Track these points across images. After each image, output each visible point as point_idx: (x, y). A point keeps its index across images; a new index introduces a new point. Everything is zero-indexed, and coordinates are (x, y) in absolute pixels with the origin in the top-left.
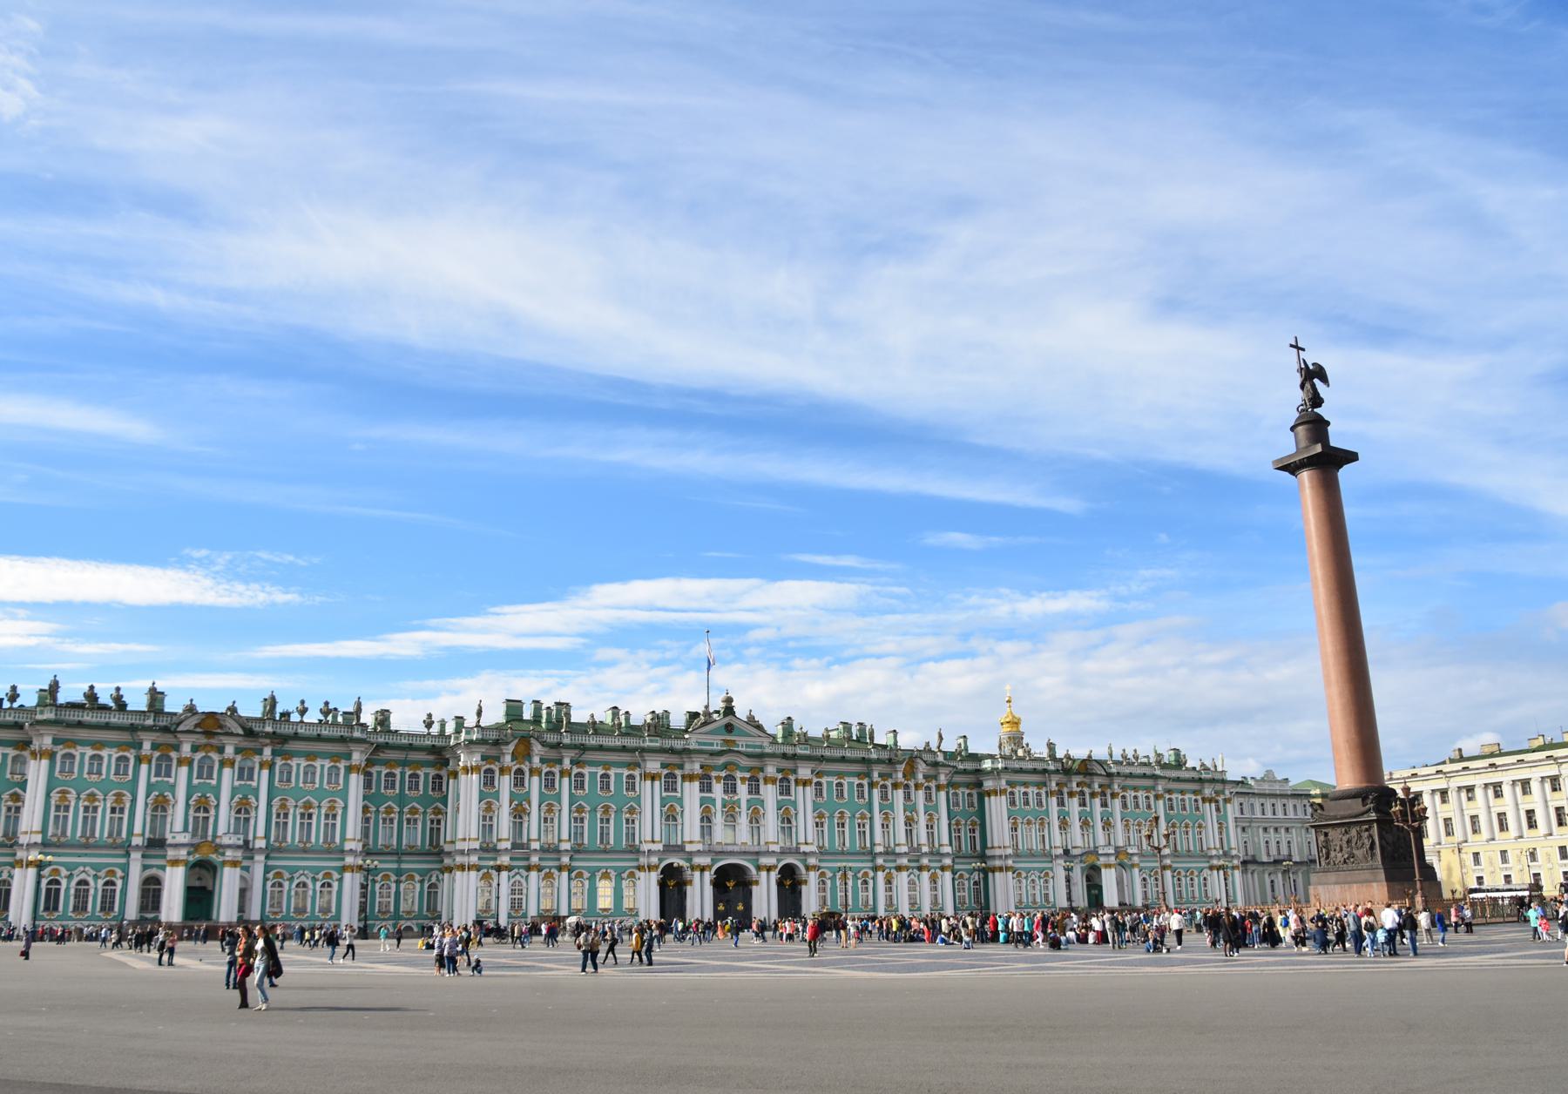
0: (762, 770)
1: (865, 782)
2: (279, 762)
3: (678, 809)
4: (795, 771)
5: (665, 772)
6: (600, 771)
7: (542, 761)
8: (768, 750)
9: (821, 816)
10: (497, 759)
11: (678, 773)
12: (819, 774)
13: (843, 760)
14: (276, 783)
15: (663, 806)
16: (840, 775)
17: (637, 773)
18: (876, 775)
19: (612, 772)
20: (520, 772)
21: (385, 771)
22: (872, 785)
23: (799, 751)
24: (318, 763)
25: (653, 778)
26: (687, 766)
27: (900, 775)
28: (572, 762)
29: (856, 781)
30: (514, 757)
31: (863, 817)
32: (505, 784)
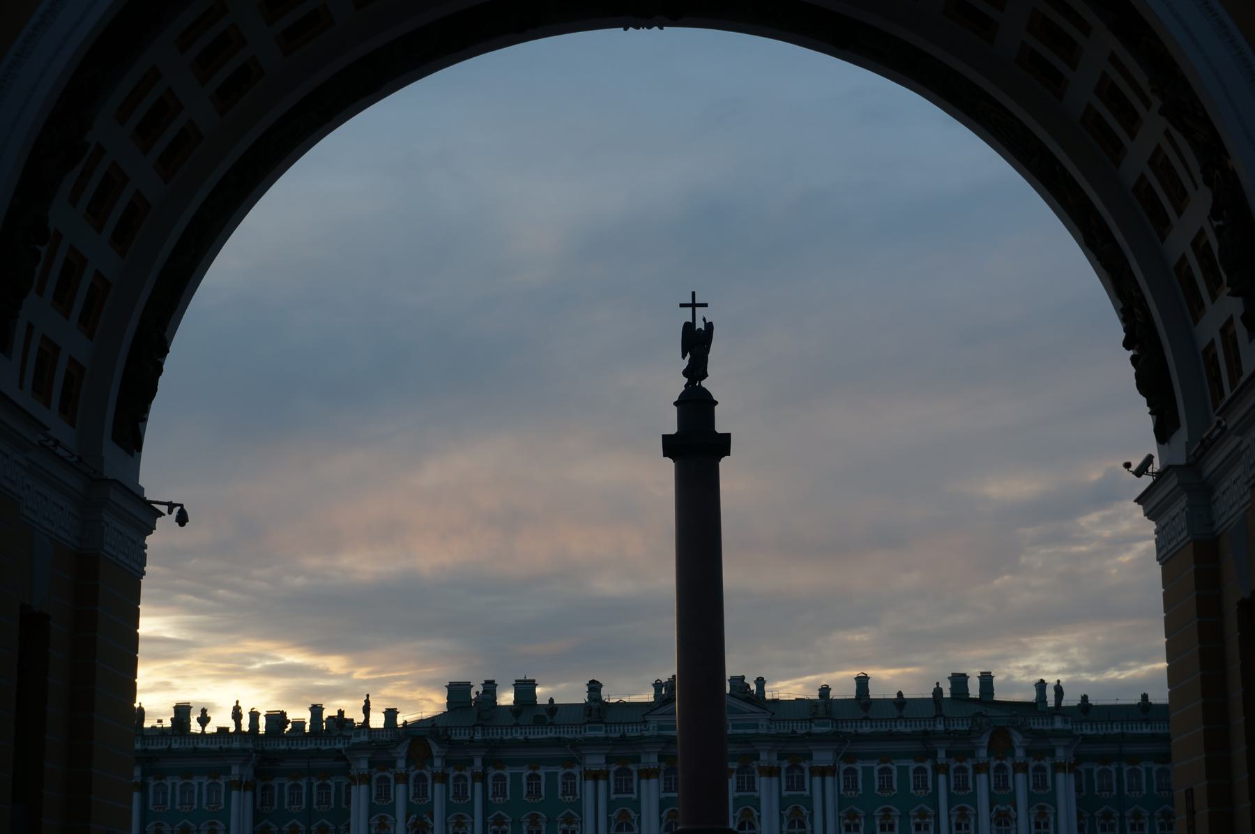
0: (757, 757)
1: (928, 765)
2: (152, 783)
3: (633, 814)
4: (809, 757)
5: (614, 768)
6: (526, 772)
7: (448, 763)
8: (763, 731)
9: (852, 815)
10: (392, 764)
11: (632, 767)
12: (850, 758)
13: (891, 736)
14: (151, 807)
15: (610, 810)
16: (886, 757)
17: (576, 771)
18: (941, 755)
19: (541, 772)
20: (421, 778)
21: (288, 784)
22: (937, 769)
23: (816, 729)
24: (195, 781)
25: (596, 776)
26: (643, 759)
27: (983, 753)
28: (486, 763)
29: (913, 765)
30: (410, 760)
31: (923, 814)
32: (400, 794)
